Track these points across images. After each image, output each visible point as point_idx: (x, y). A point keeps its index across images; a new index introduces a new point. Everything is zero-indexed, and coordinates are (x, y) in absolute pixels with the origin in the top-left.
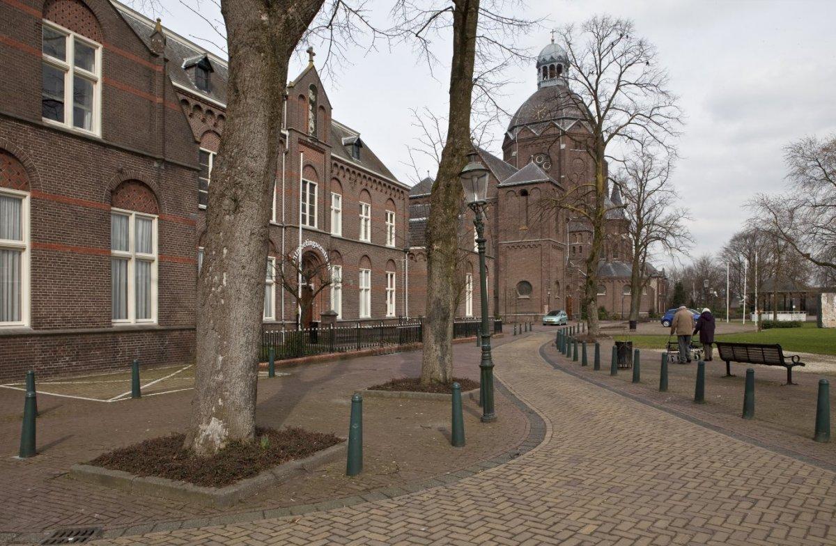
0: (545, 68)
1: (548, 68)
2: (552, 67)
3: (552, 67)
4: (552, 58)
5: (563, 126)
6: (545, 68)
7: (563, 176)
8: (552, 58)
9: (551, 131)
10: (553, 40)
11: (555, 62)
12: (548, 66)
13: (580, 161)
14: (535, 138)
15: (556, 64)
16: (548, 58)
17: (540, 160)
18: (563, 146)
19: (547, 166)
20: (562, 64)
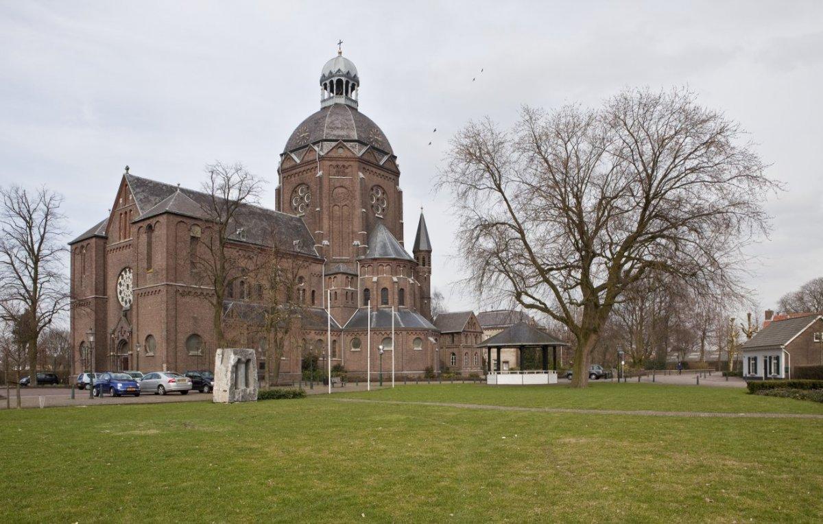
0: (325, 85)
1: (328, 85)
2: (331, 82)
3: (331, 82)
4: (331, 72)
5: (322, 149)
6: (325, 85)
7: (318, 209)
8: (331, 72)
9: (310, 157)
10: (340, 53)
11: (333, 76)
12: (328, 82)
13: (344, 189)
14: (296, 166)
15: (334, 80)
16: (327, 75)
17: (302, 191)
18: (320, 173)
19: (308, 198)
20: (344, 79)
